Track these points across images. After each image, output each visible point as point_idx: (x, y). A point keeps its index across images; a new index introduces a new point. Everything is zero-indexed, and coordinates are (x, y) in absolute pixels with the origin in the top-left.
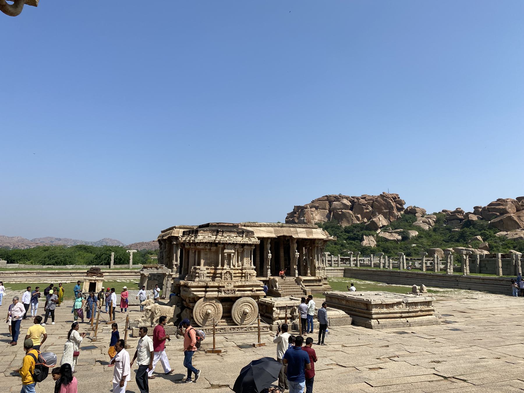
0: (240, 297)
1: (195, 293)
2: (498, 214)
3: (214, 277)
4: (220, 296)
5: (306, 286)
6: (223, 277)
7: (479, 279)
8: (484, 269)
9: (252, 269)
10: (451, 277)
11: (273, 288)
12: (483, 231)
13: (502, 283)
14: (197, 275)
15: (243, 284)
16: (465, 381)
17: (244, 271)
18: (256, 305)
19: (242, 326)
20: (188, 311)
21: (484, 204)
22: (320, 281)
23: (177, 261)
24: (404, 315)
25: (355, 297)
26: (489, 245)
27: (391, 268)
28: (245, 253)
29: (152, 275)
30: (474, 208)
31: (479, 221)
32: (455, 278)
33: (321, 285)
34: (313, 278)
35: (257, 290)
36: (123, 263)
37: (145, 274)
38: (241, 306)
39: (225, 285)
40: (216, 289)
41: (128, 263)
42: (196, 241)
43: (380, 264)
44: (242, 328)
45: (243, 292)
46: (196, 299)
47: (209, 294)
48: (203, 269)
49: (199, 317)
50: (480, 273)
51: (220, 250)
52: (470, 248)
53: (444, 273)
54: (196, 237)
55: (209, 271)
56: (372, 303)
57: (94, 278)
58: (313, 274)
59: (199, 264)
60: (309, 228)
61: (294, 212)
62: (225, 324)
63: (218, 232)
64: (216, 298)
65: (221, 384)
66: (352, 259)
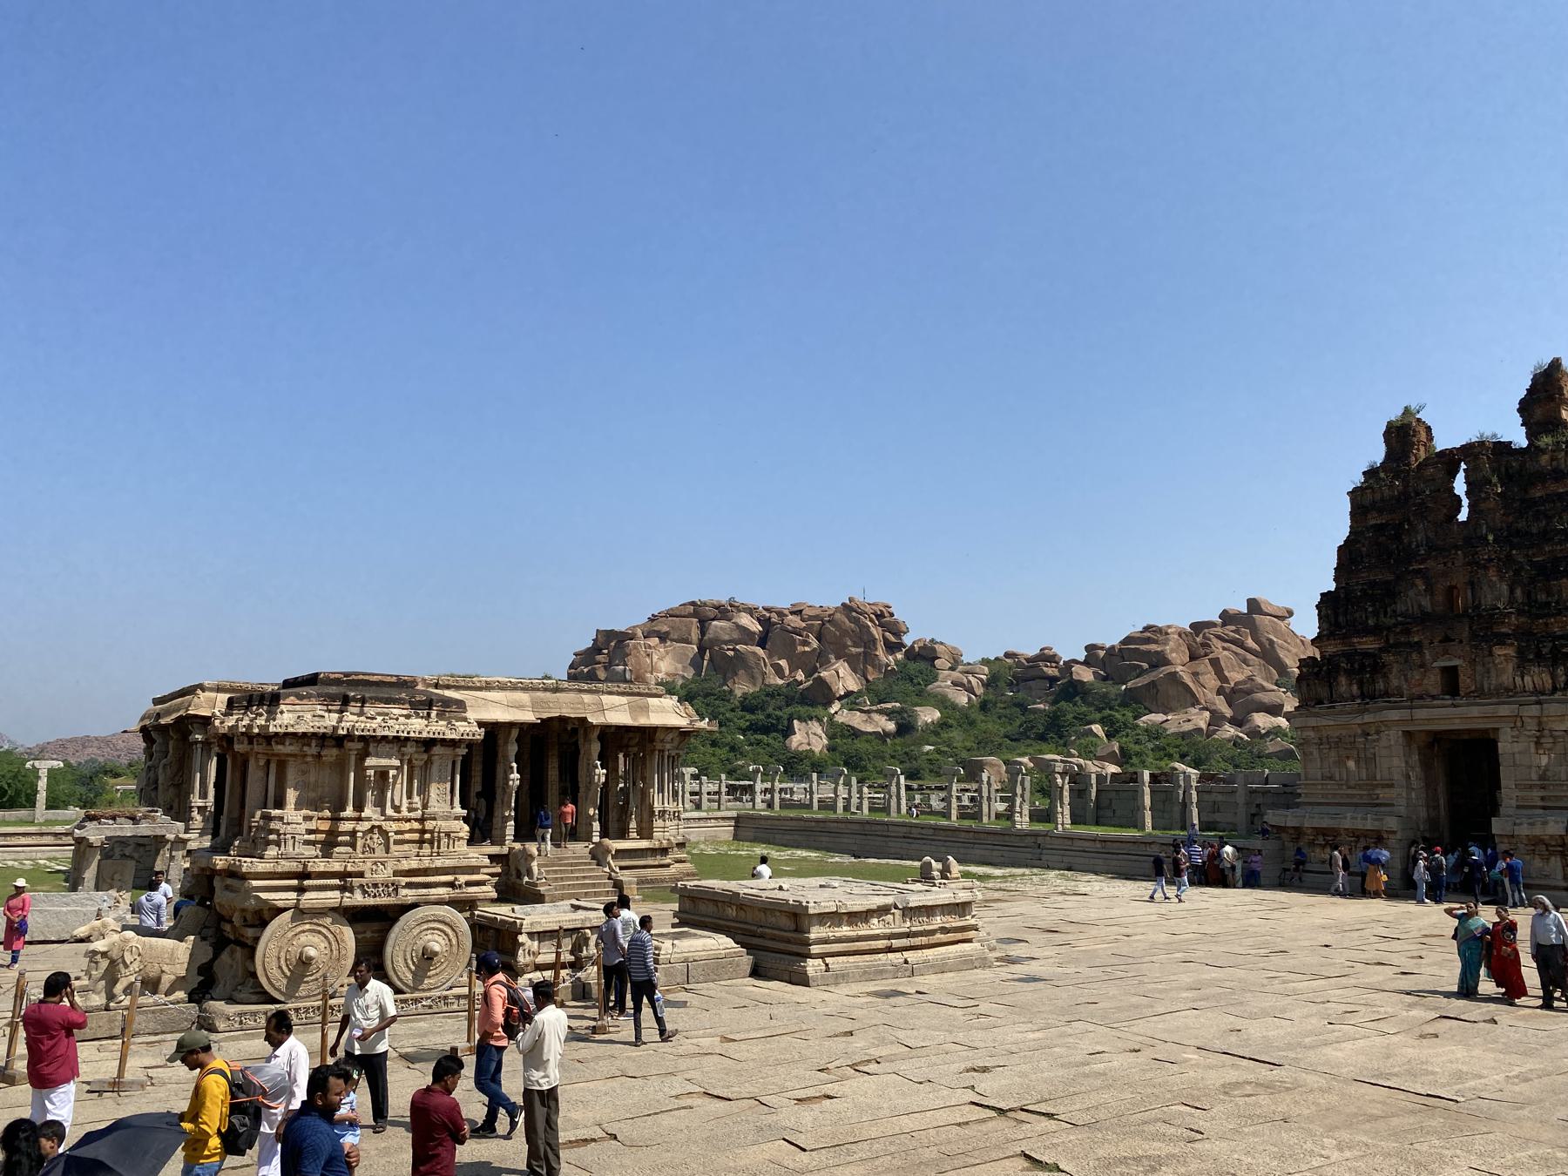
0: (415, 906)
3: (328, 845)
4: (347, 902)
5: (622, 868)
6: (360, 843)
7: (1094, 840)
8: (1109, 813)
9: (457, 818)
10: (1024, 835)
11: (519, 876)
12: (1107, 712)
15: (426, 863)
17: (429, 825)
20: (239, 952)
21: (1111, 638)
22: (664, 851)
23: (204, 795)
24: (896, 943)
25: (764, 894)
26: (1121, 748)
27: (866, 811)
28: (435, 768)
33: (668, 866)
34: (644, 844)
35: (469, 884)
37: (92, 839)
38: (415, 932)
39: (366, 867)
40: (336, 882)
42: (272, 729)
43: (835, 801)
44: (416, 1001)
45: (424, 891)
46: (263, 916)
47: (311, 899)
48: (294, 818)
50: (1097, 824)
52: (1073, 756)
53: (1005, 824)
54: (271, 715)
55: (312, 825)
56: (811, 911)
58: (646, 833)
59: (280, 803)
60: (639, 694)
61: (596, 649)
63: (346, 701)
64: (333, 909)
66: (759, 786)
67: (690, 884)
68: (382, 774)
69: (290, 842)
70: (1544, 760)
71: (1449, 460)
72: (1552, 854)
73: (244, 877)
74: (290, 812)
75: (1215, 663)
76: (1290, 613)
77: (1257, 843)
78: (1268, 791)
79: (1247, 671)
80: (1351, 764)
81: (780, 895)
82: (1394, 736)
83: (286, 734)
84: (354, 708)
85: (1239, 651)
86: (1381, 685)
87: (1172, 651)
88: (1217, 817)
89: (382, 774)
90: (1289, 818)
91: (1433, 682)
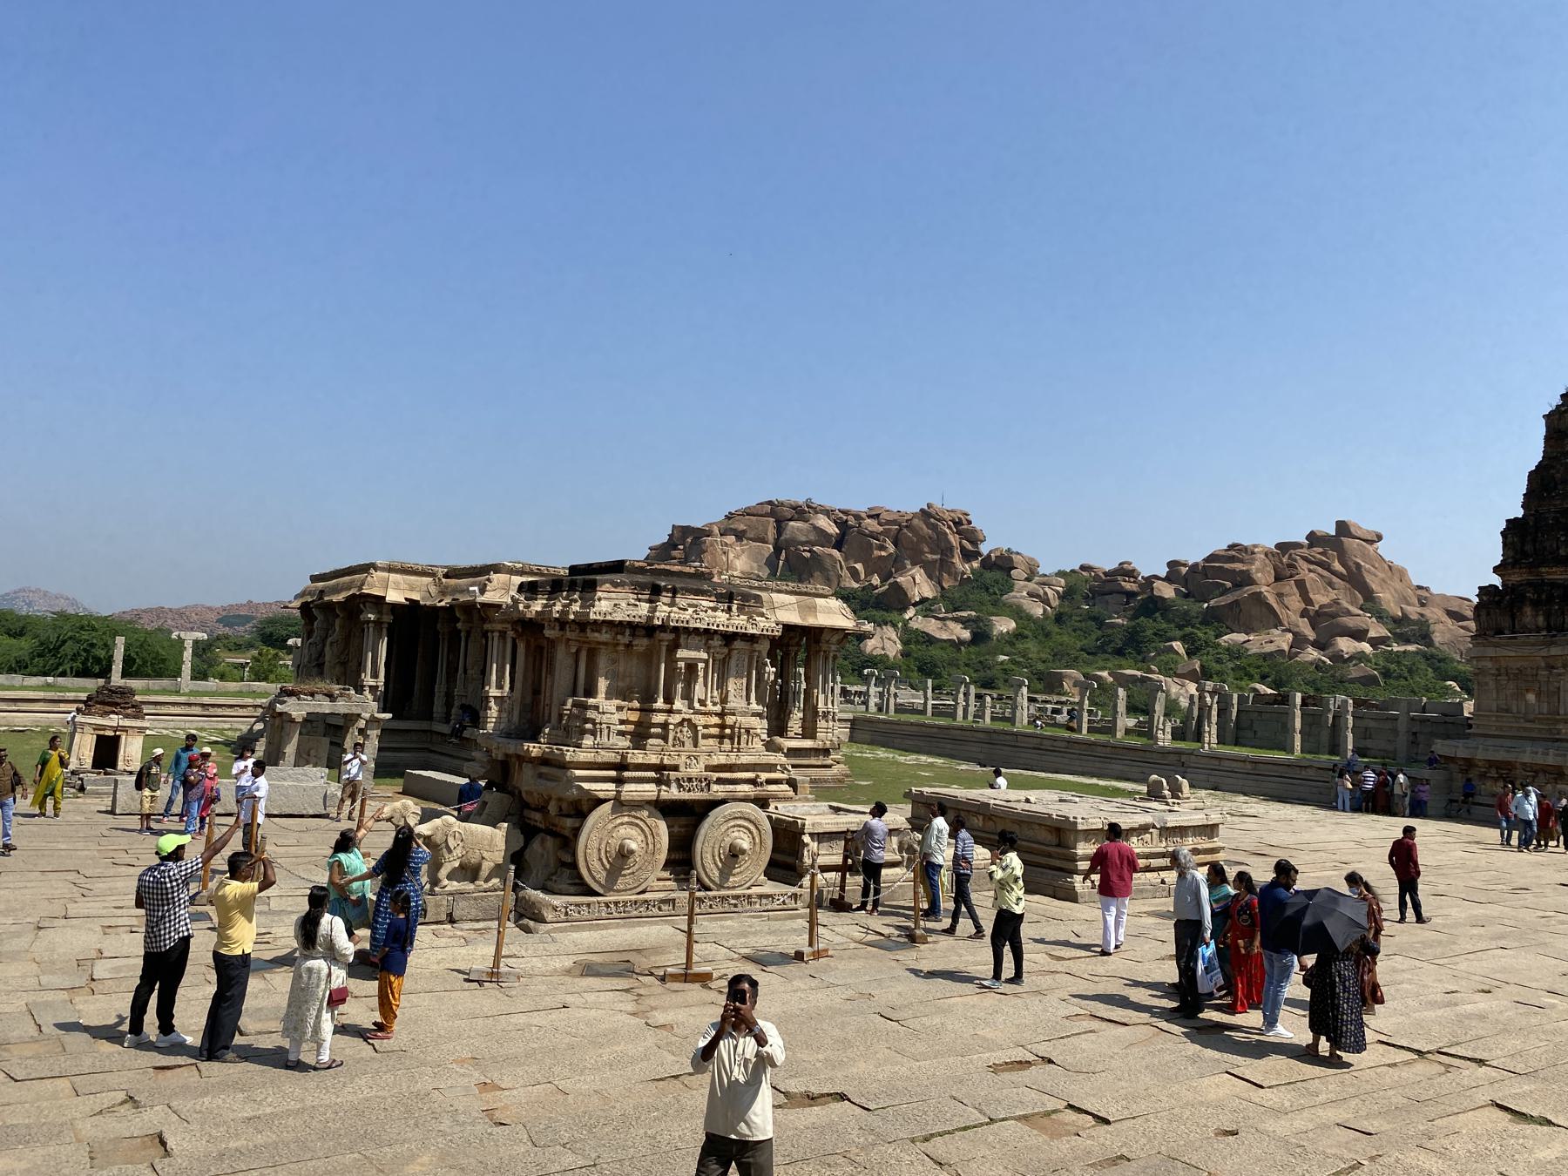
2: (1229, 584)
3: (640, 736)
4: (664, 795)
5: (794, 766)
7: (1245, 760)
8: (1250, 734)
9: (754, 715)
10: (1165, 752)
12: (1189, 630)
13: (1304, 774)
14: (589, 726)
15: (733, 759)
16: (1481, 1062)
17: (730, 720)
18: (767, 826)
19: (723, 892)
20: (550, 842)
21: (1194, 555)
22: (826, 752)
23: (375, 675)
26: (1202, 666)
27: (988, 719)
28: (733, 663)
29: (311, 719)
30: (1170, 564)
31: (1180, 601)
32: (1176, 757)
33: (829, 766)
34: (808, 744)
35: (769, 782)
36: (159, 674)
38: (723, 828)
39: (681, 761)
40: (652, 774)
41: (178, 673)
42: (592, 616)
43: (955, 706)
44: (724, 899)
45: (731, 787)
47: (631, 791)
48: (609, 710)
49: (596, 865)
52: (1153, 672)
54: (588, 602)
56: (1080, 827)
57: (114, 720)
58: (809, 731)
59: (591, 691)
60: (806, 594)
63: (656, 591)
64: (649, 802)
65: (815, 1090)
66: (873, 690)
67: (926, 790)
68: (691, 667)
73: (565, 766)
74: (600, 699)
75: (1301, 585)
76: (1380, 538)
77: (1426, 773)
78: (1428, 720)
79: (1333, 595)
81: (1027, 807)
84: (665, 598)
85: (1325, 573)
87: (1258, 571)
88: (1369, 743)
89: (691, 667)
90: (1459, 749)
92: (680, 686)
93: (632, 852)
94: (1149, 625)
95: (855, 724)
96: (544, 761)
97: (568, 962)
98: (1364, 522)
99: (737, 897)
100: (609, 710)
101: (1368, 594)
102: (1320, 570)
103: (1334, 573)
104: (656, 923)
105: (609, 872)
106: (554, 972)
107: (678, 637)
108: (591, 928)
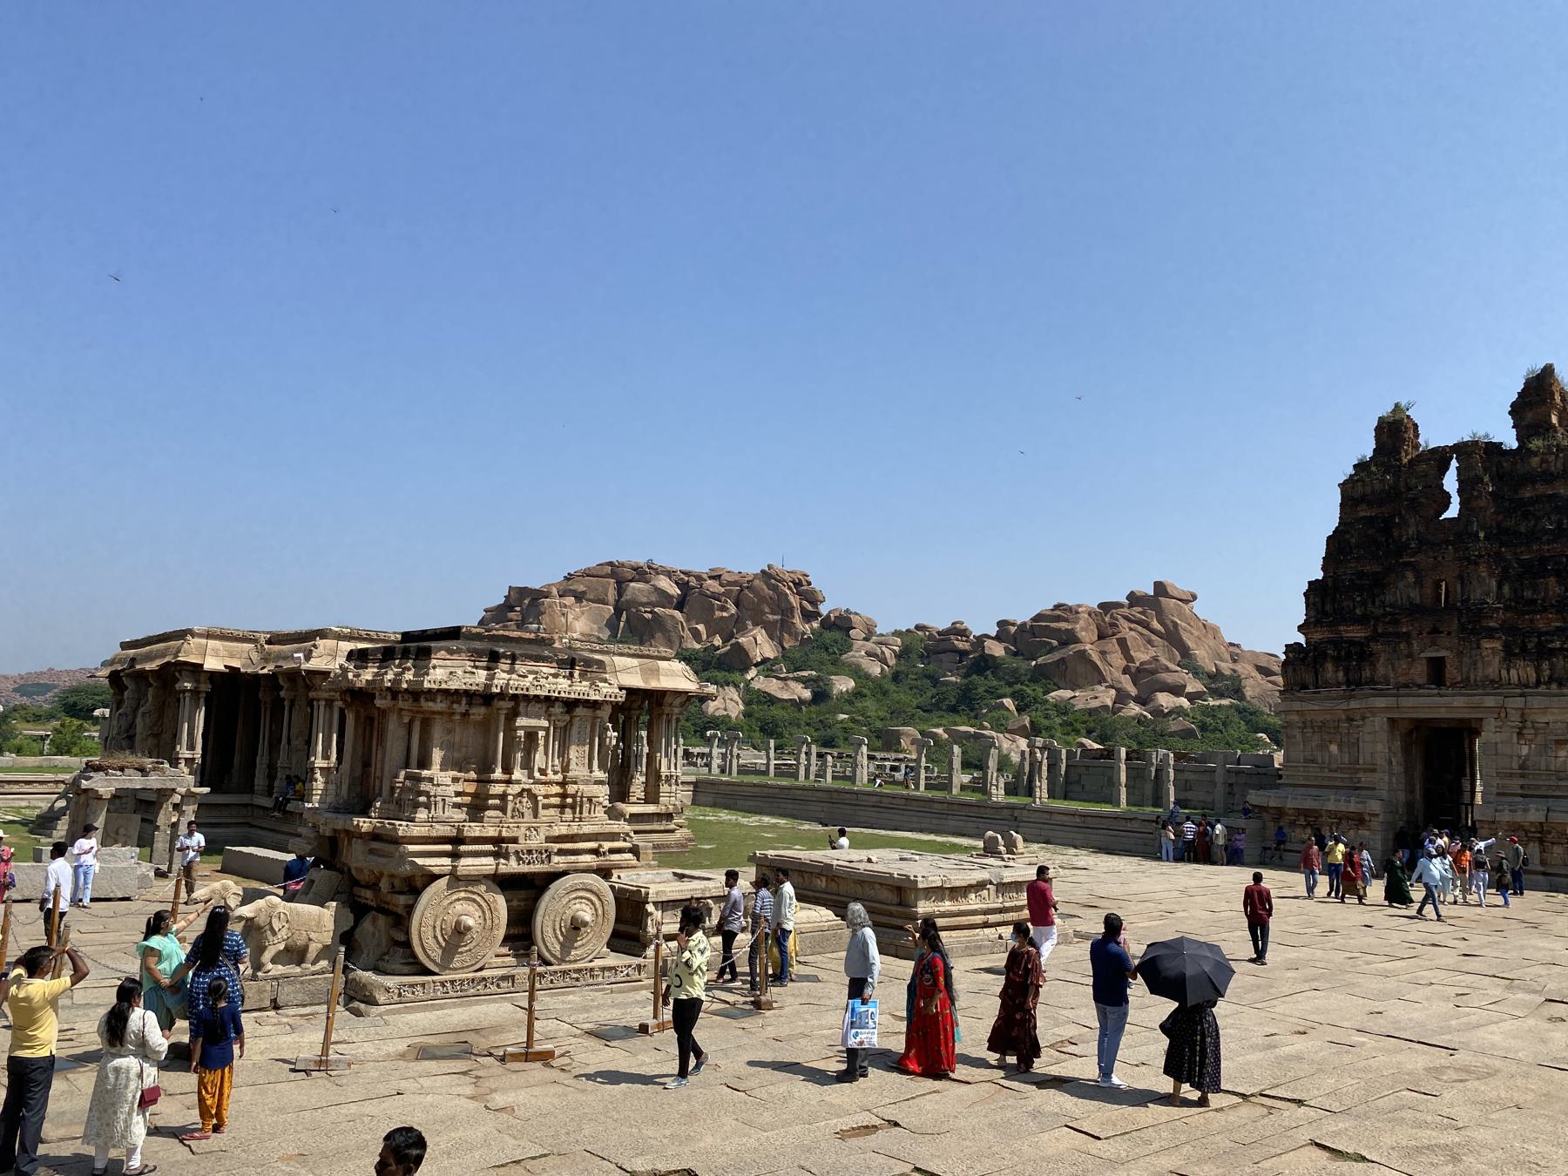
0: (565, 873)
1: (420, 861)
3: (477, 808)
4: (503, 869)
6: (510, 806)
7: (1074, 814)
8: (1077, 788)
10: (999, 808)
13: (1129, 826)
14: (422, 799)
17: (571, 789)
18: (610, 897)
19: (564, 967)
20: (382, 921)
21: (1022, 614)
23: (191, 747)
24: (992, 918)
25: (835, 863)
26: (1032, 722)
29: (118, 796)
31: (1009, 659)
33: (672, 831)
34: (651, 809)
35: (612, 851)
37: (101, 790)
40: (490, 847)
42: (426, 685)
44: (564, 973)
46: (417, 883)
47: (467, 865)
48: (445, 782)
49: (430, 942)
50: (1065, 798)
51: (502, 718)
53: (972, 798)
54: (422, 671)
56: (920, 886)
58: (651, 796)
59: (424, 763)
60: (648, 657)
61: (507, 606)
62: (511, 960)
63: (494, 658)
64: (486, 876)
66: (716, 751)
67: (771, 853)
68: (531, 735)
69: (440, 805)
70: (1525, 750)
71: (1440, 458)
72: (1530, 840)
73: (398, 841)
74: (434, 771)
75: (1123, 643)
76: (1194, 597)
77: (1241, 822)
79: (1152, 652)
80: (1334, 748)
81: (869, 867)
82: (1378, 723)
83: (439, 690)
84: (504, 665)
86: (1367, 673)
87: (1082, 629)
88: (1189, 795)
89: (531, 735)
90: (1270, 799)
91: (1419, 672)
92: (519, 755)
93: (469, 929)
94: (981, 683)
95: (697, 786)
96: (375, 836)
97: (401, 1046)
98: (1179, 582)
99: (579, 971)
100: (445, 782)
101: (1185, 651)
102: (1140, 628)
103: (1153, 631)
104: (495, 1001)
105: (444, 950)
106: (388, 1057)
107: (517, 704)
108: (426, 1009)
